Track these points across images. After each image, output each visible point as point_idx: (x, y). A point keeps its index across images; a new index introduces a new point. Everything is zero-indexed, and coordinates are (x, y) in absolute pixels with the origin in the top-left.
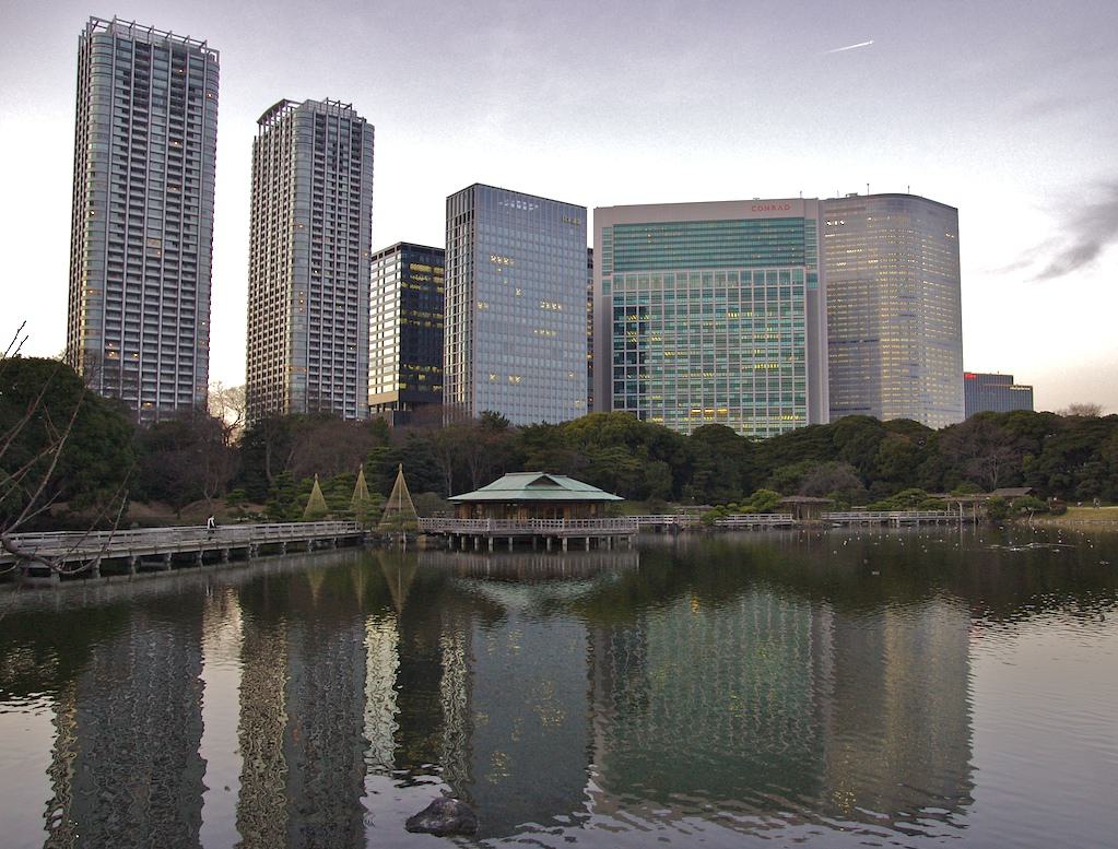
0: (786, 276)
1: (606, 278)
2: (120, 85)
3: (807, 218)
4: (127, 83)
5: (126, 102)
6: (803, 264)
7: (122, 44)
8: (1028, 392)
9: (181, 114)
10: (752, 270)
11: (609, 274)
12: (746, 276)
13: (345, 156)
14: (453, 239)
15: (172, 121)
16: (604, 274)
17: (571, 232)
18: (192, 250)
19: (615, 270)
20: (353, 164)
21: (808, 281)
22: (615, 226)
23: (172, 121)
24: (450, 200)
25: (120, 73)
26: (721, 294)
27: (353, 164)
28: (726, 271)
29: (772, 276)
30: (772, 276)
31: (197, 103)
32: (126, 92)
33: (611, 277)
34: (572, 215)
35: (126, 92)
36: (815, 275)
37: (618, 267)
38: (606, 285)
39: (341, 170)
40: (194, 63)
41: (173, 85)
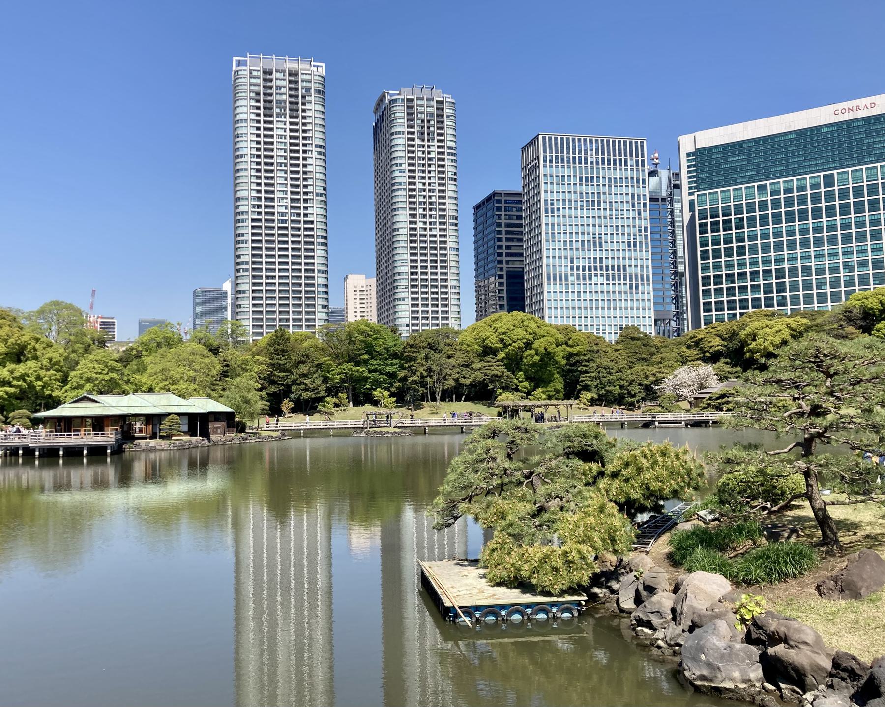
1: (692, 197)
2: (254, 103)
4: (258, 101)
5: (258, 115)
7: (254, 73)
9: (297, 117)
13: (432, 129)
15: (291, 124)
16: (690, 194)
18: (310, 218)
20: (438, 134)
23: (291, 124)
25: (253, 95)
27: (438, 134)
31: (308, 106)
32: (258, 108)
33: (694, 197)
35: (258, 108)
39: (429, 141)
40: (304, 77)
41: (291, 96)
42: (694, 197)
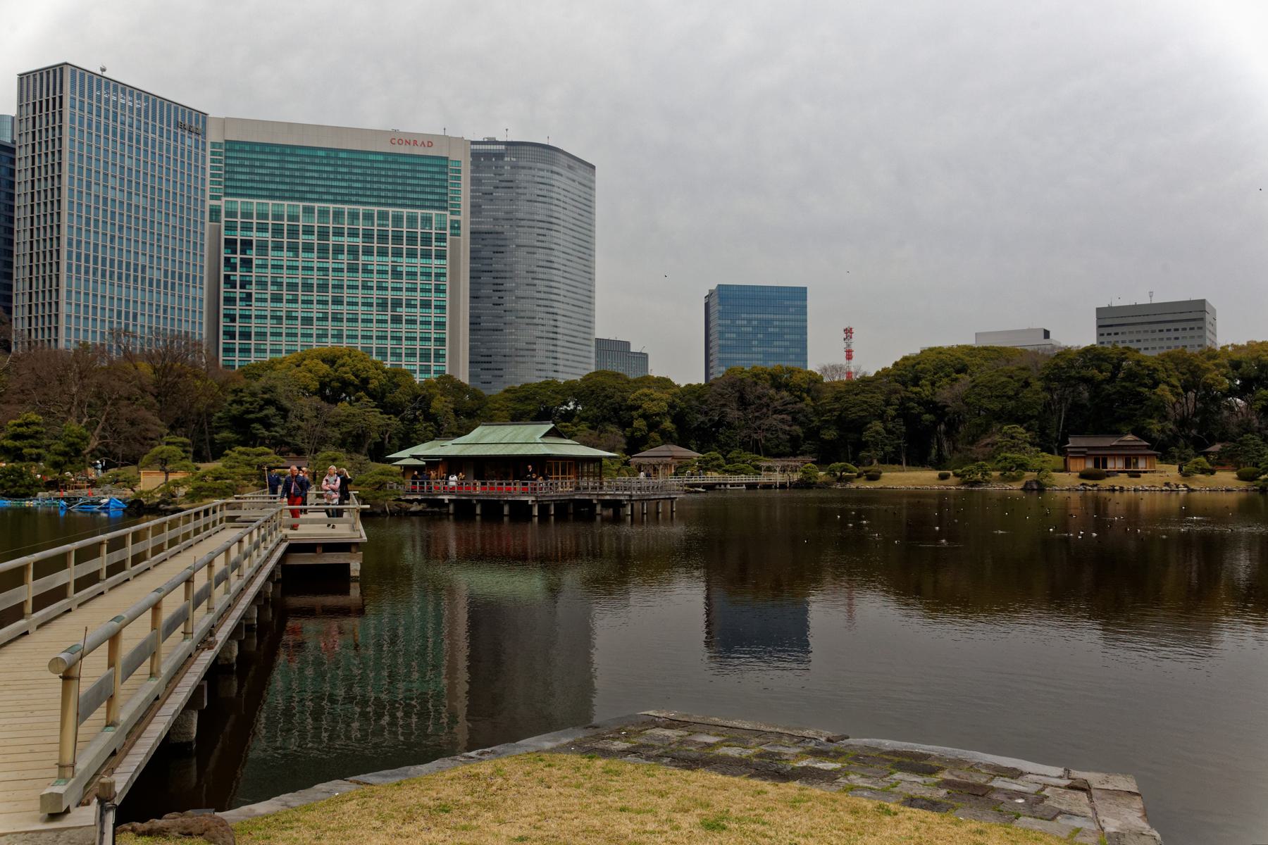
0: (427, 220)
3: (451, 158)
6: (446, 209)
8: (643, 357)
10: (391, 210)
11: (218, 198)
12: (383, 216)
14: (31, 130)
16: (212, 197)
17: (187, 141)
19: (226, 194)
21: (452, 228)
22: (227, 141)
24: (22, 77)
26: (353, 233)
28: (361, 209)
29: (412, 220)
30: (412, 220)
33: (222, 203)
34: (190, 122)
36: (458, 222)
37: (230, 191)
38: (215, 212)
42: (222, 203)
